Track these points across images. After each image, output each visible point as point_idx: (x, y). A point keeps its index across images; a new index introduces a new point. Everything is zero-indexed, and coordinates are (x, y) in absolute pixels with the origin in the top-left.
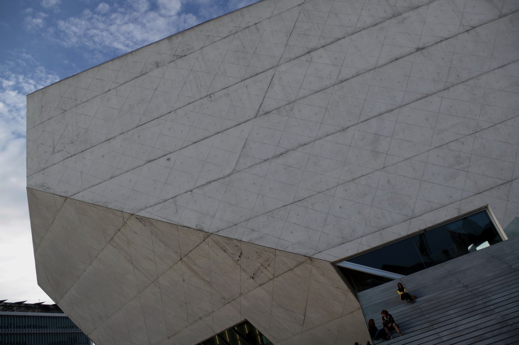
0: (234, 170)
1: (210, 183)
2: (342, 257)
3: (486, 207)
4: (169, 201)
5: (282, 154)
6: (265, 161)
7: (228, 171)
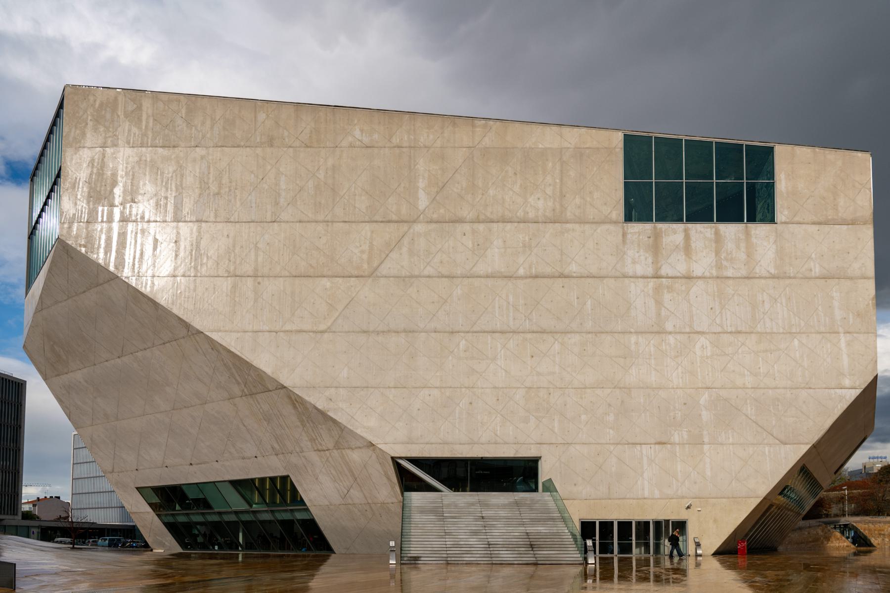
0: (329, 328)
2: (404, 455)
3: (540, 458)
6: (365, 332)
7: (322, 327)
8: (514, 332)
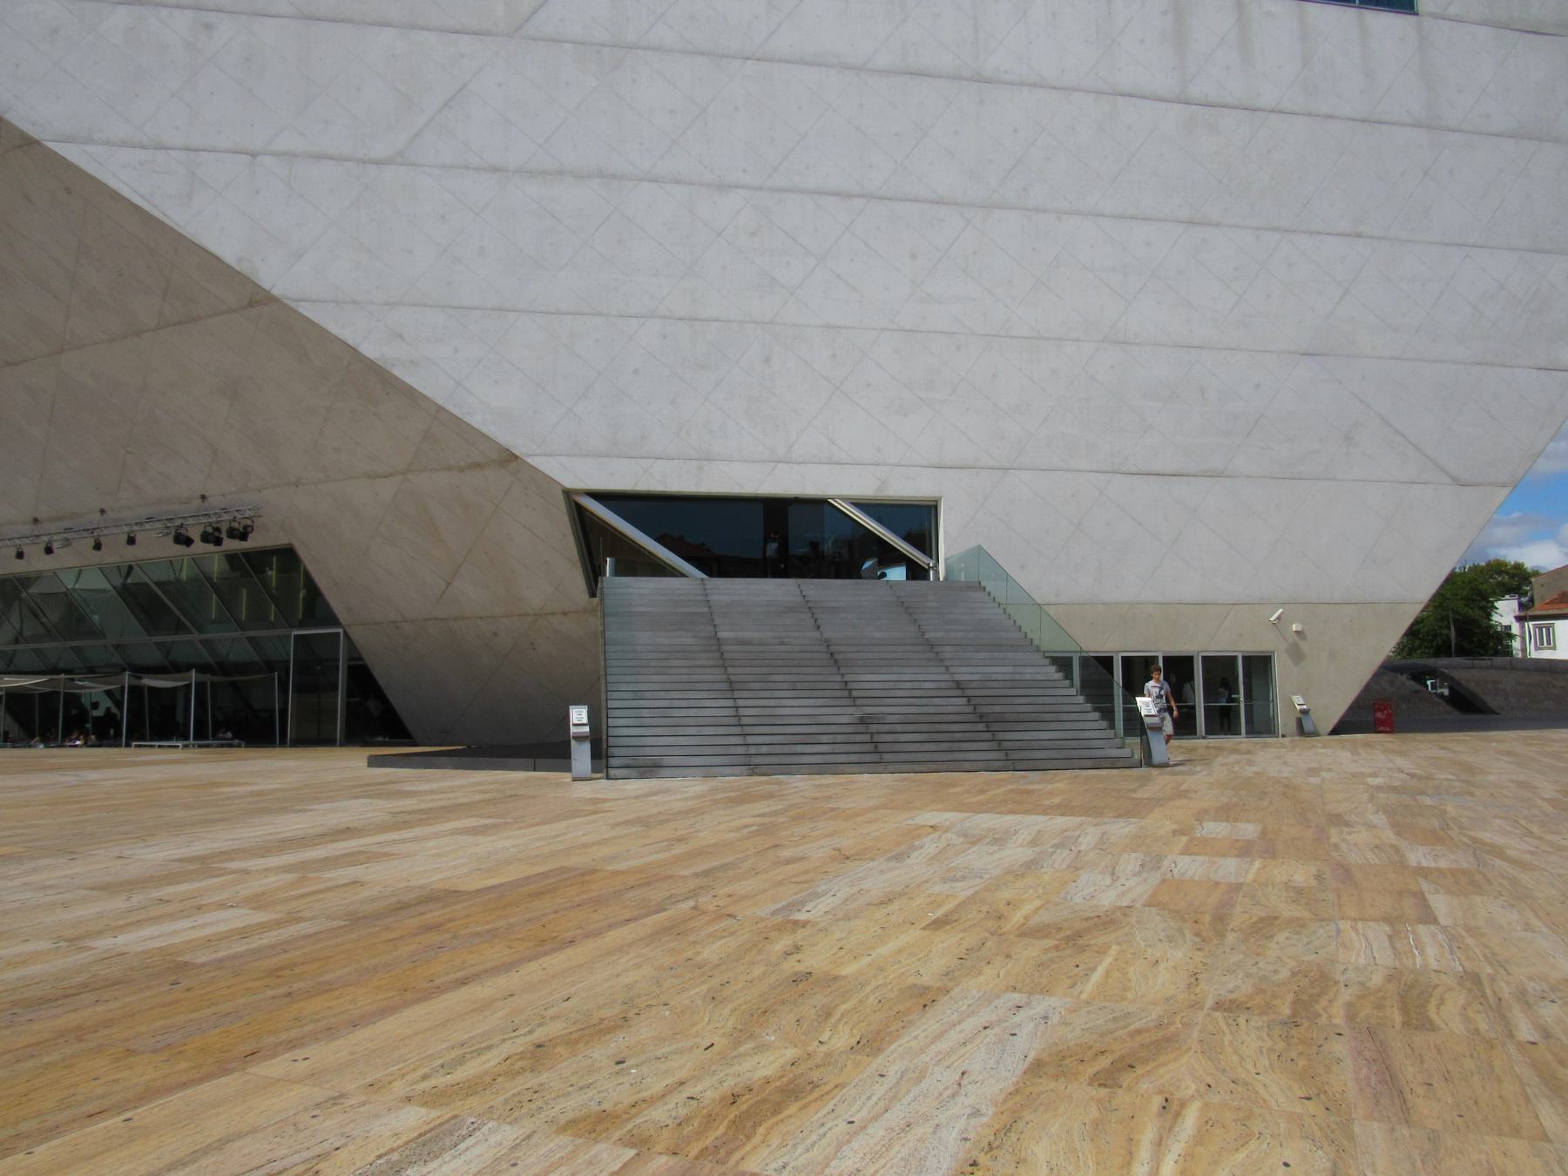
1: (320, 157)
4: (174, 153)
5: (544, 173)
6: (496, 169)
8: (871, 197)
